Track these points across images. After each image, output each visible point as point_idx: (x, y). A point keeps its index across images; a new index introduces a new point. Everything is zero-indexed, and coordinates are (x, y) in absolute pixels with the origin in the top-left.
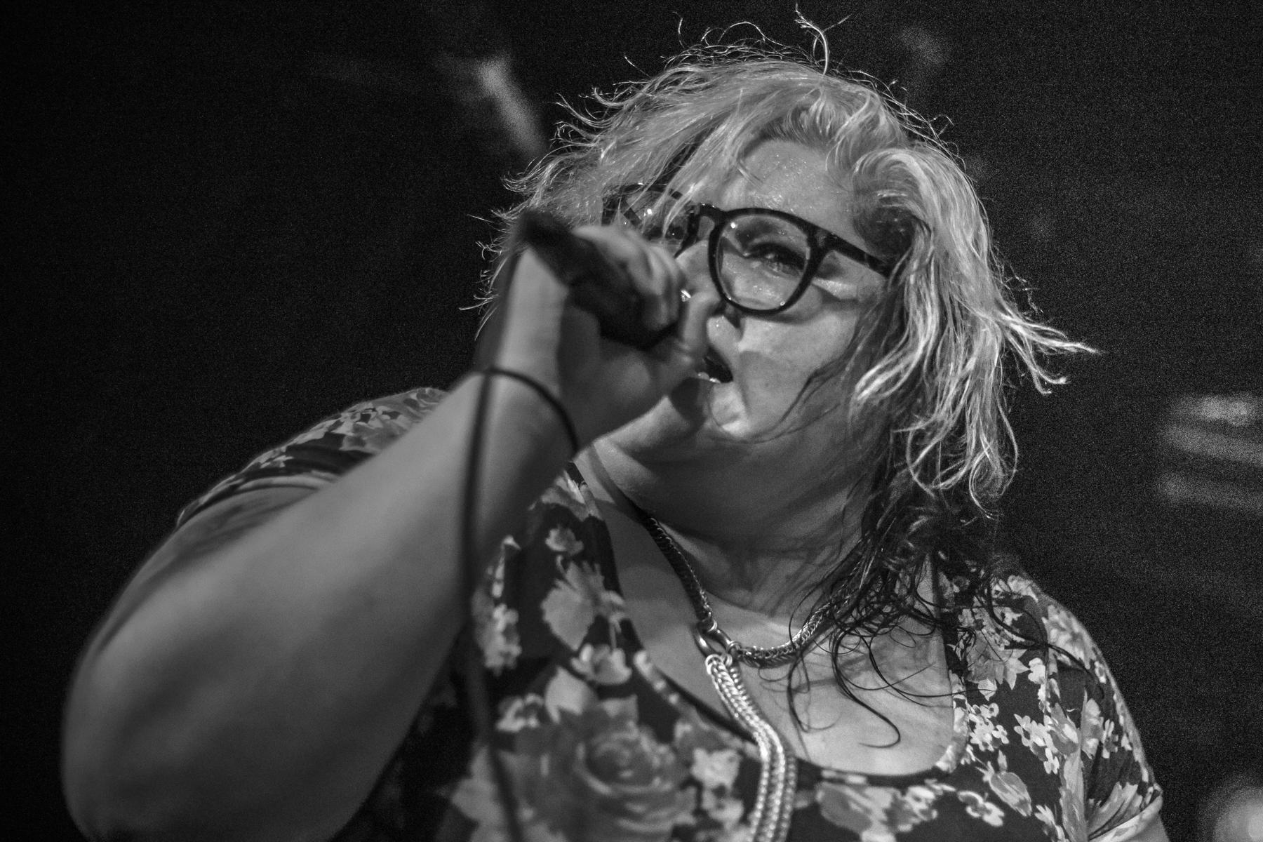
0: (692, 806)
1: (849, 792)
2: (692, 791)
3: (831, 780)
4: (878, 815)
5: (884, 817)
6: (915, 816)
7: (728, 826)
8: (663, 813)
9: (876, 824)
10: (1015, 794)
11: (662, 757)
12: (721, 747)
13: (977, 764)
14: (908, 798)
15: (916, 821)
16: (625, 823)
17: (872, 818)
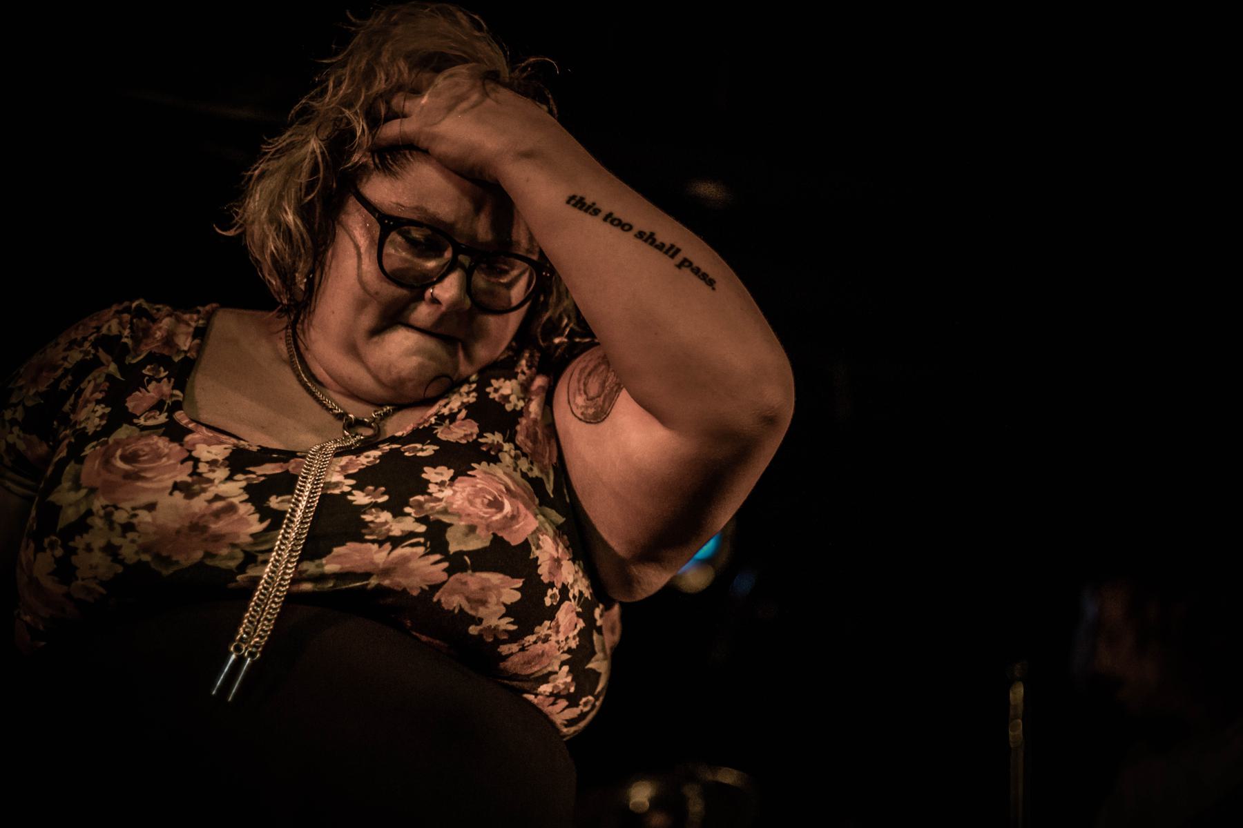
7: (216, 482)
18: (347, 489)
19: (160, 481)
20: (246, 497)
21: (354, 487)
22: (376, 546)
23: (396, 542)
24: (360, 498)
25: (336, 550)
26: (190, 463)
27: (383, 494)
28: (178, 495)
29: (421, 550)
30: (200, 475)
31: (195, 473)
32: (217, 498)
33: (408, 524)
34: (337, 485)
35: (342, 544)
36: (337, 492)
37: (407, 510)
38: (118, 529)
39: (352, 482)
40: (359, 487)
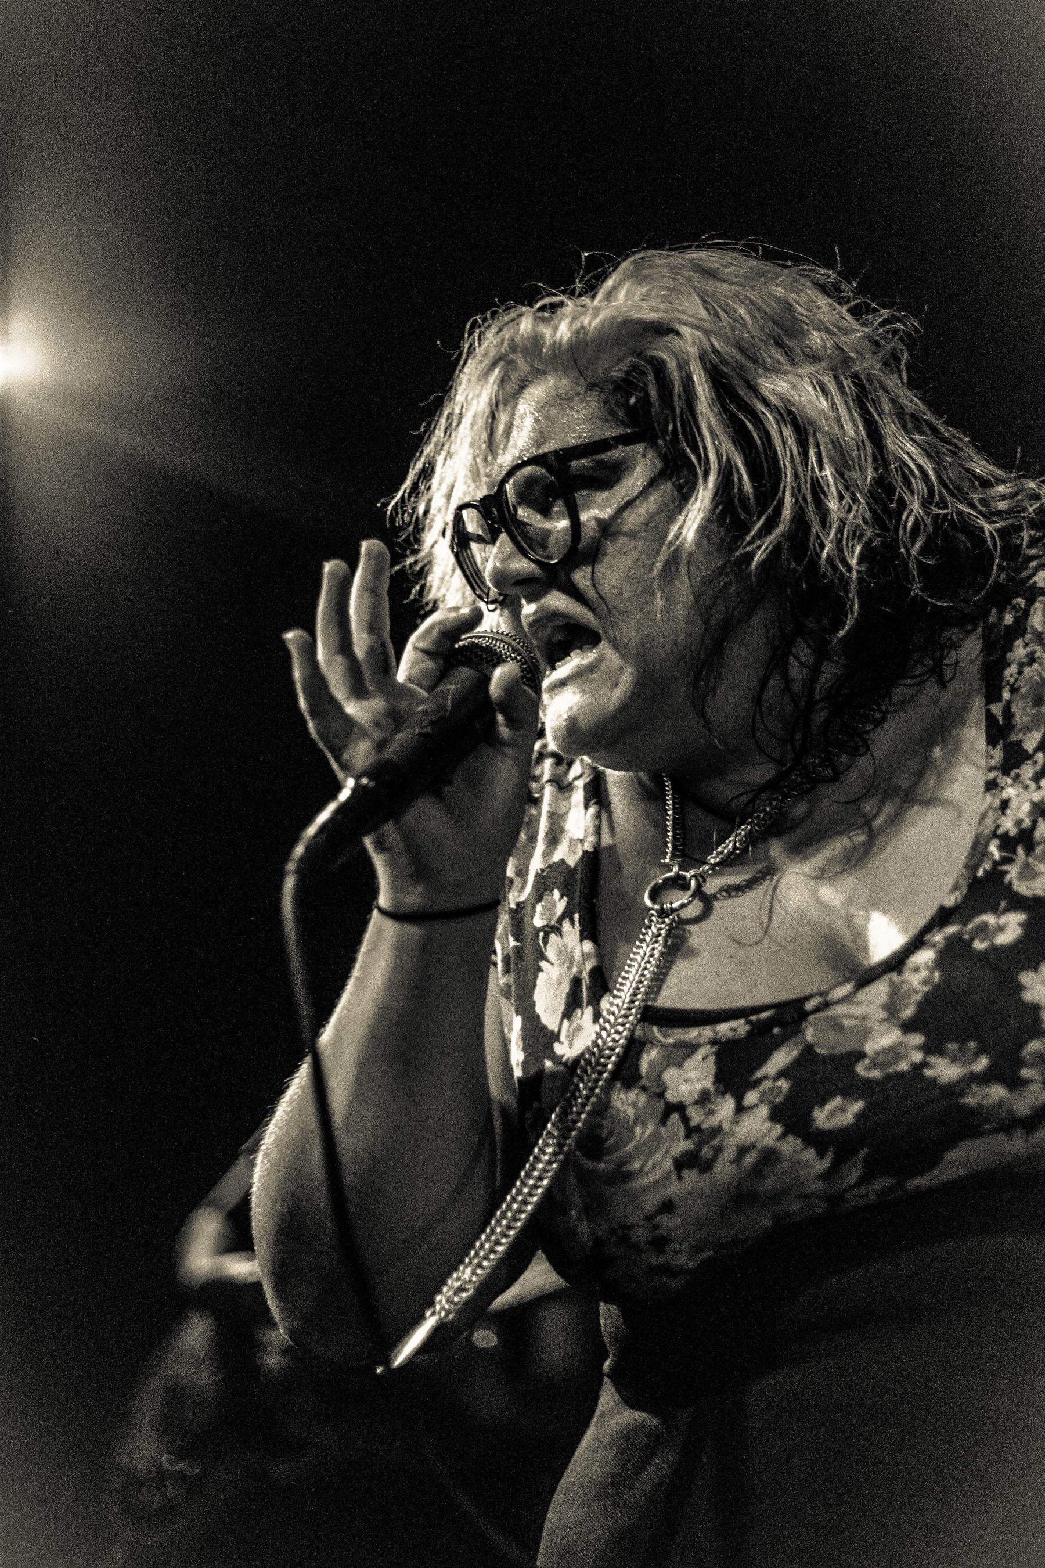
0: (682, 1132)
2: (675, 1117)
3: (817, 1010)
5: (883, 1014)
6: (916, 991)
7: (726, 1126)
8: (658, 1156)
9: (875, 1026)
11: (634, 1104)
12: (691, 1048)
13: (1005, 861)
15: (917, 997)
16: (631, 1185)
17: (869, 1023)
18: (918, 1057)
19: (654, 1166)
20: (778, 1129)
21: (928, 1049)
24: (945, 1070)
25: (950, 1156)
26: (675, 1117)
27: (978, 1054)
28: (691, 1176)
30: (698, 1129)
31: (691, 1132)
32: (743, 1151)
34: (896, 1052)
36: (904, 1066)
37: (1026, 1073)
40: (932, 1048)
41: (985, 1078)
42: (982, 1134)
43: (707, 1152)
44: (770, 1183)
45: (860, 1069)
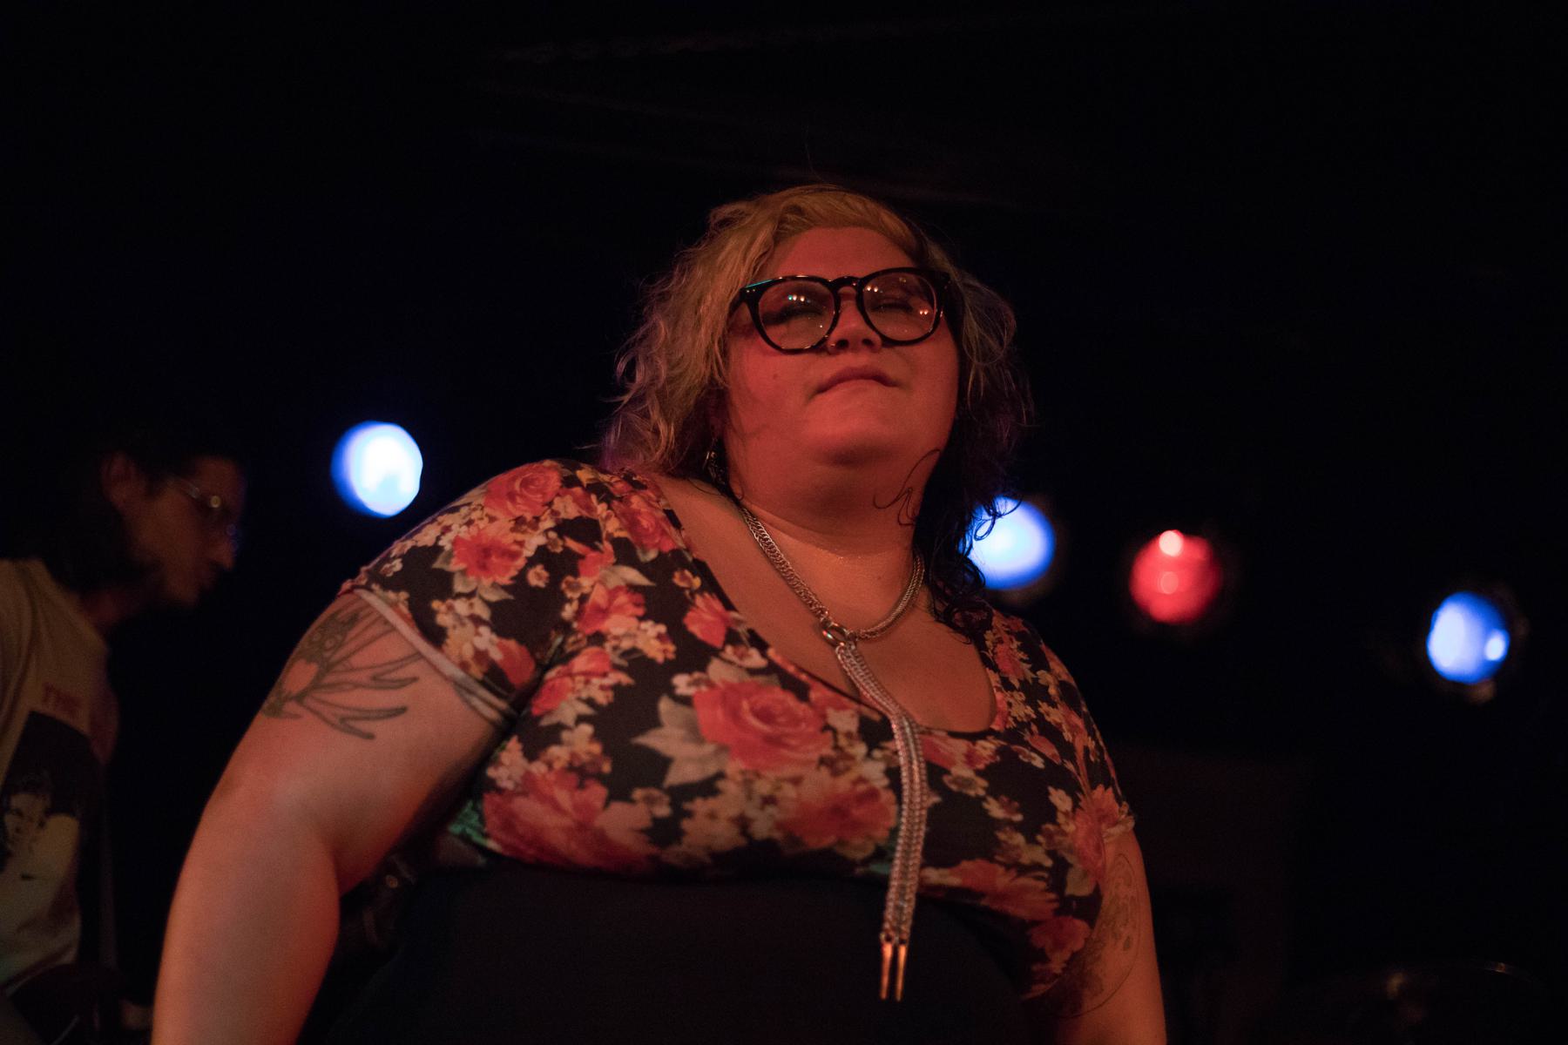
0: (832, 743)
1: (937, 742)
4: (960, 758)
7: (859, 758)
8: (811, 747)
10: (1050, 751)
14: (978, 747)
16: (784, 752)
18: (982, 793)
22: (1001, 870)
23: (1023, 870)
24: (995, 809)
27: (1018, 811)
28: (825, 772)
29: (1042, 885)
33: (1036, 854)
34: (969, 783)
35: (970, 858)
36: (972, 793)
37: (1040, 838)
38: (757, 801)
39: (983, 783)
40: (993, 791)
41: (1018, 827)
42: (991, 860)
43: (841, 765)
44: (857, 812)
45: (946, 779)
